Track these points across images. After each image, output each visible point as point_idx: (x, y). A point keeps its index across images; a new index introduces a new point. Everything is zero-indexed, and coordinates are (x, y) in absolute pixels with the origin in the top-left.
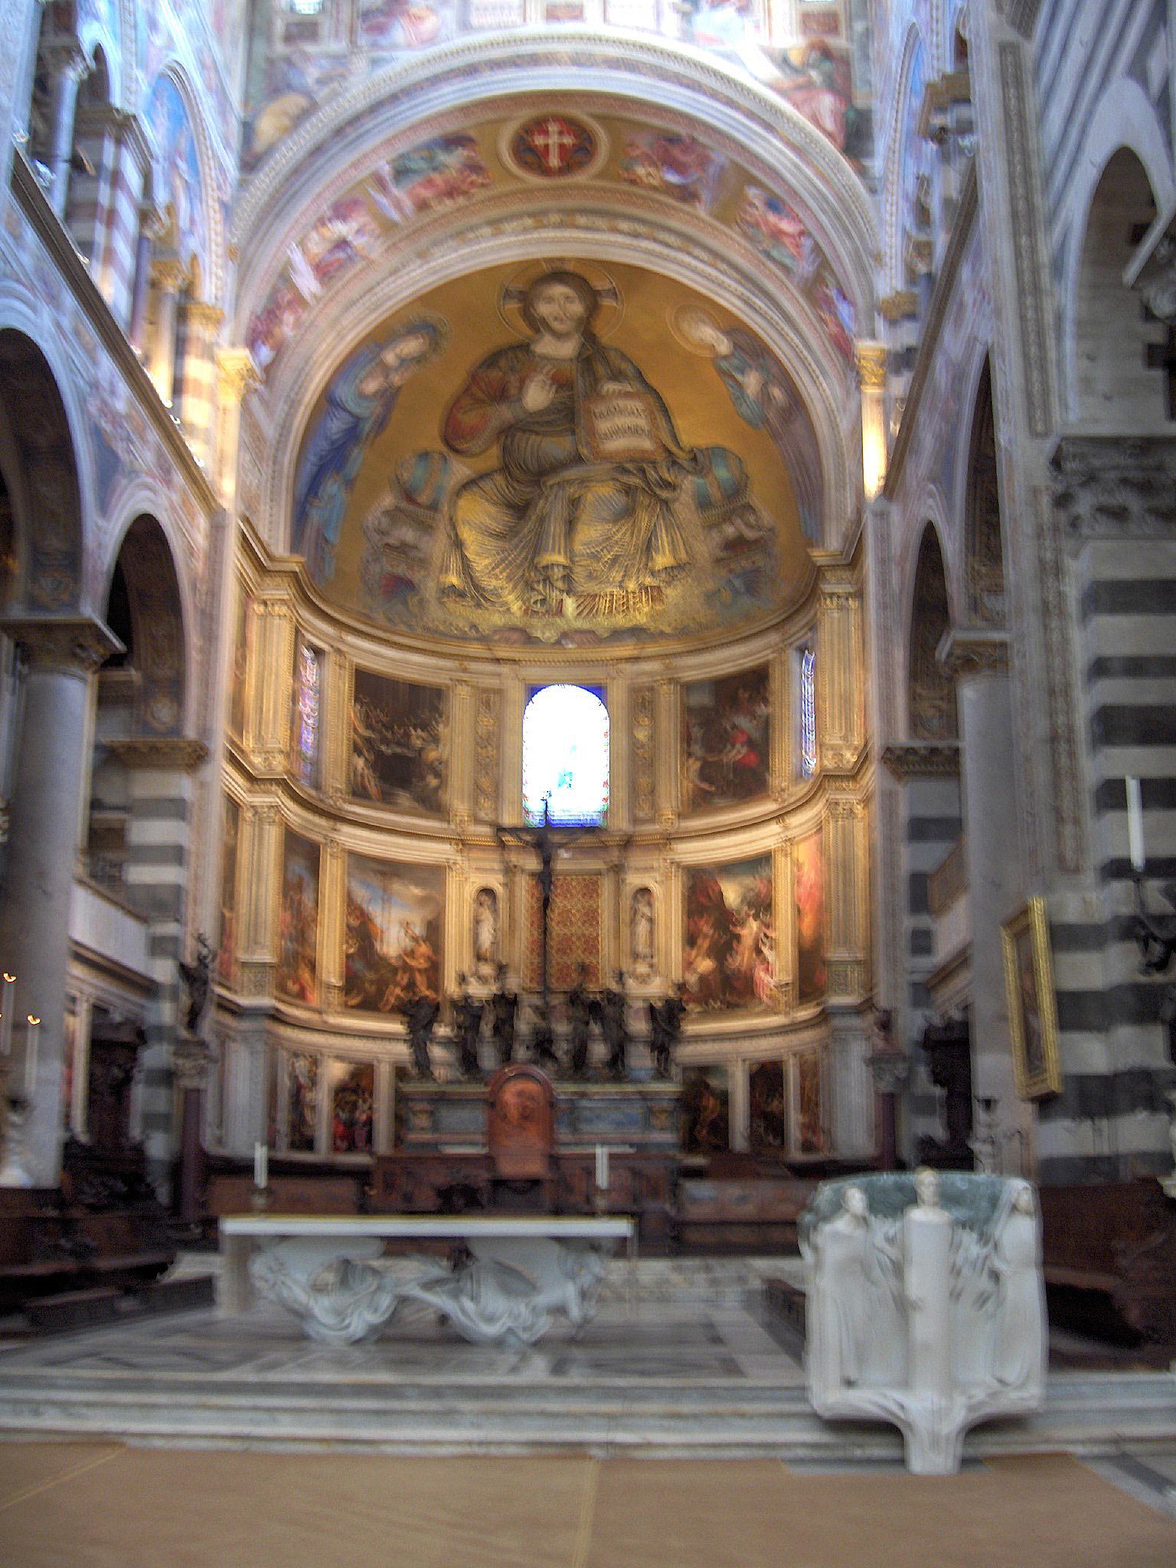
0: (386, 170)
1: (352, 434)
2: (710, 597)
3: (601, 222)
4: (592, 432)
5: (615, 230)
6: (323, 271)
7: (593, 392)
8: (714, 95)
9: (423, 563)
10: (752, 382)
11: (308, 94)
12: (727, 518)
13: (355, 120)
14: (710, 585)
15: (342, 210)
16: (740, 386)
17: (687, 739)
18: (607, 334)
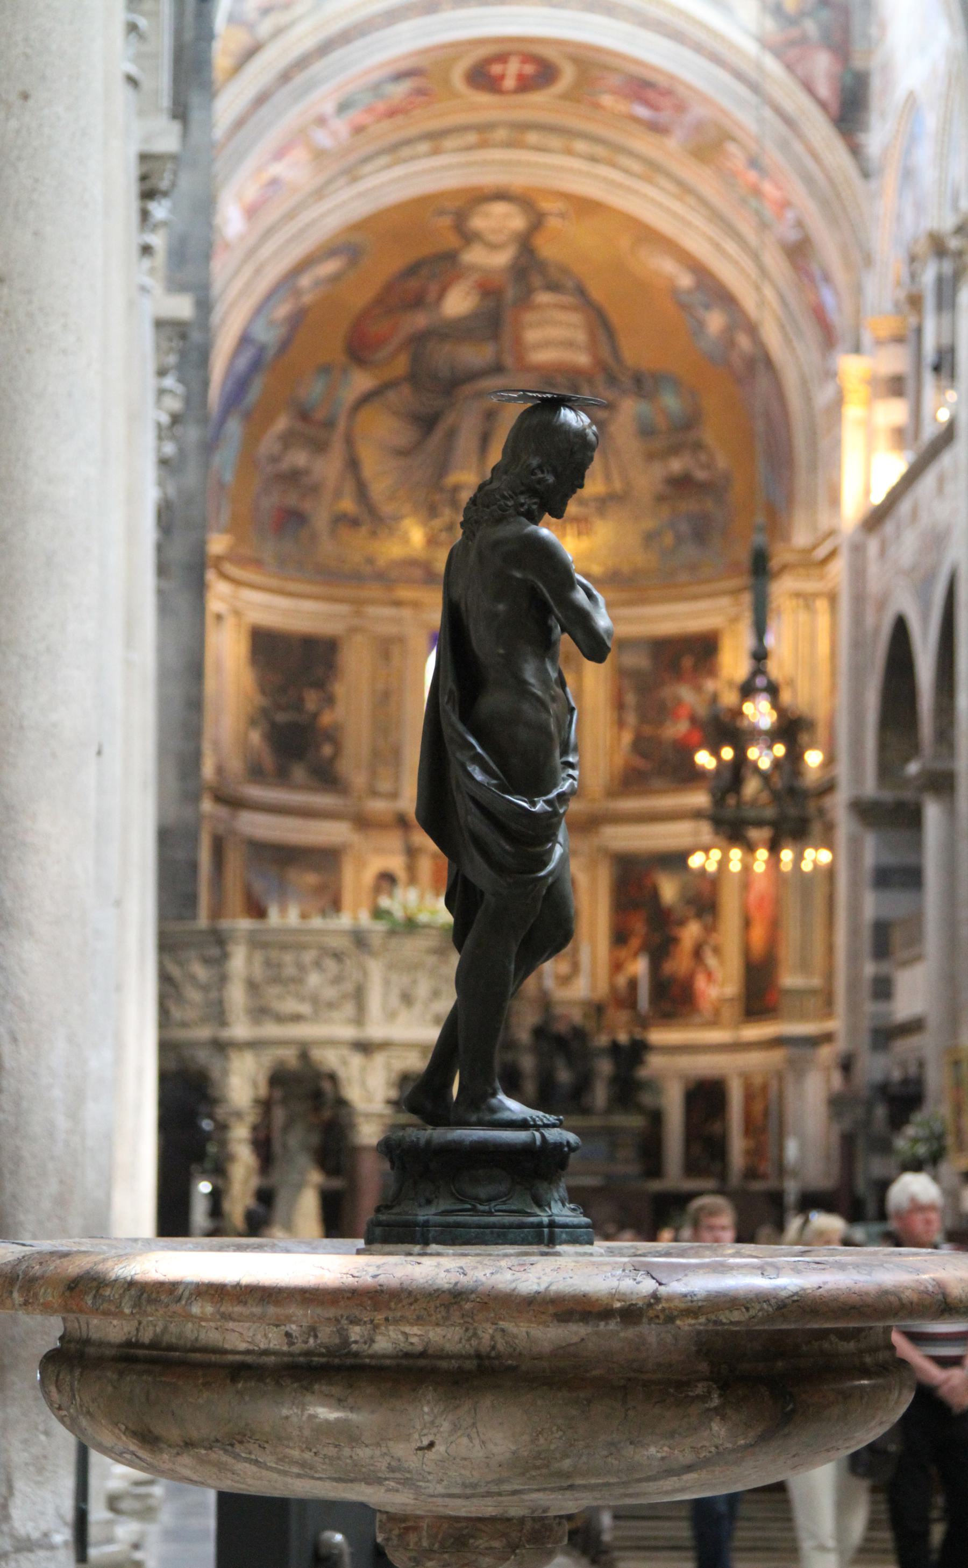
0: (329, 107)
1: (256, 366)
2: (650, 538)
3: (555, 142)
4: (518, 341)
5: (569, 152)
6: (251, 212)
7: (524, 301)
8: (698, 48)
9: (315, 490)
10: (715, 321)
11: (250, 27)
12: (674, 450)
13: (302, 63)
14: (649, 524)
15: (280, 154)
16: (701, 324)
17: (619, 705)
18: (547, 249)
